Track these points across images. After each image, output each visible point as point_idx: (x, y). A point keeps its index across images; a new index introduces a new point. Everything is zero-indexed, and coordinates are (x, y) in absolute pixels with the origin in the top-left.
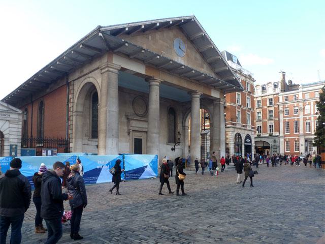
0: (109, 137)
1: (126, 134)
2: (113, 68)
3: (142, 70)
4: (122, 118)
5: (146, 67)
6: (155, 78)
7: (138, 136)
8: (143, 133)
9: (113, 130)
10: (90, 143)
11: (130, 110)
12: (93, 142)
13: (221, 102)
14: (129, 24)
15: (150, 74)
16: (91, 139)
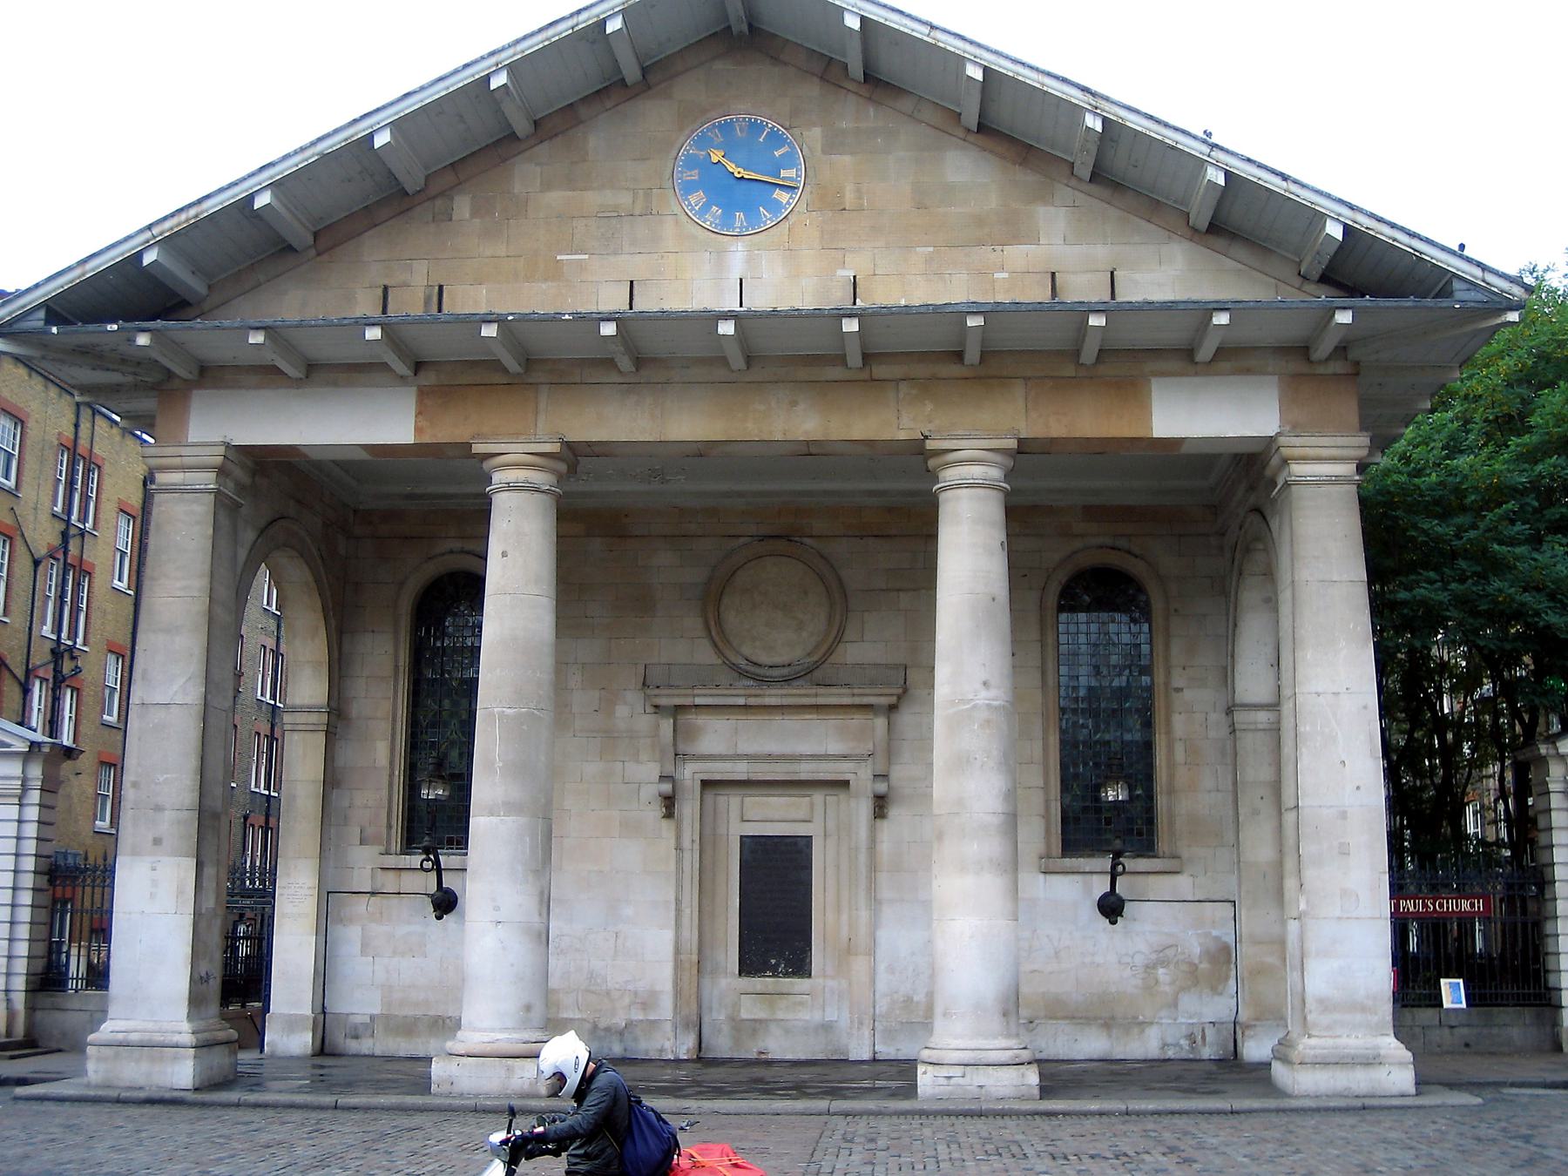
0: (136, 852)
1: (657, 810)
2: (184, 468)
3: (382, 423)
4: (622, 711)
5: (423, 394)
6: (478, 448)
7: (774, 817)
8: (818, 797)
9: (158, 808)
10: (389, 882)
11: (680, 645)
12: (405, 875)
13: (1297, 469)
14: (149, 227)
15: (447, 431)
16: (391, 861)
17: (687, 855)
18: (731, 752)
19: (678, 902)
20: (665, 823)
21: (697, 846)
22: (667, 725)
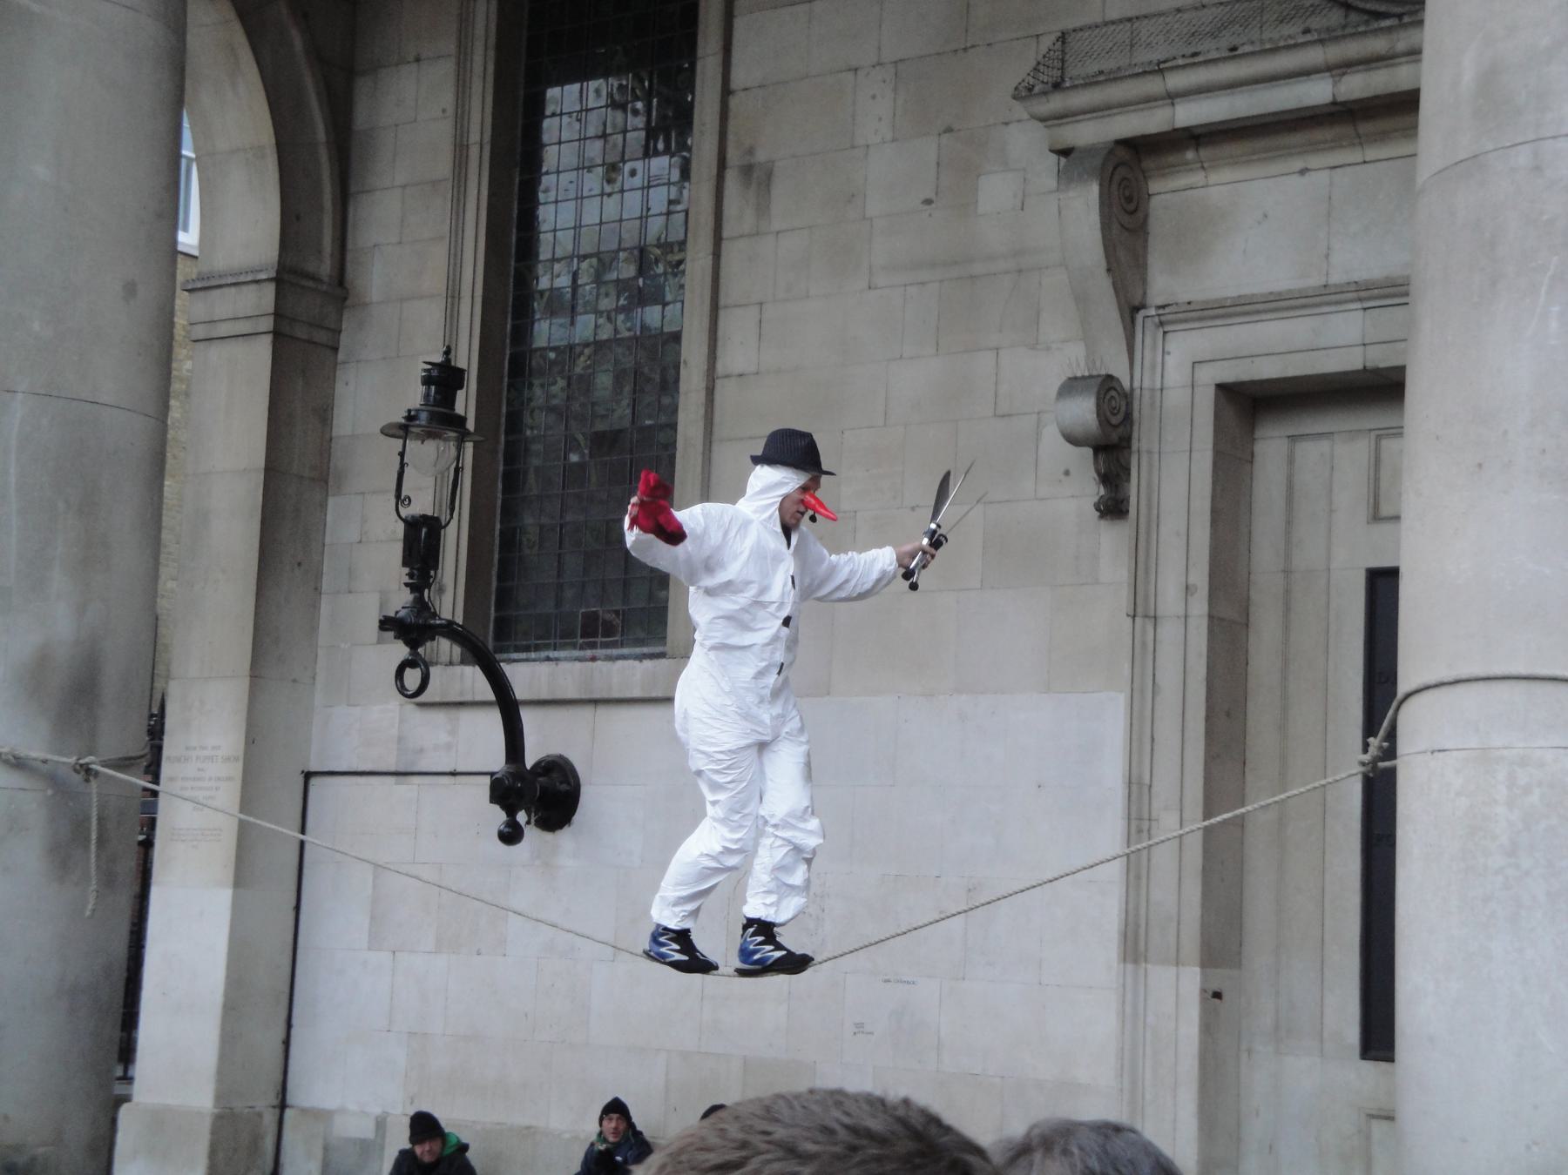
4: (996, 191)
17: (1169, 633)
18: (1315, 281)
19: (1137, 789)
20: (1112, 538)
21: (1200, 607)
22: (1082, 210)
